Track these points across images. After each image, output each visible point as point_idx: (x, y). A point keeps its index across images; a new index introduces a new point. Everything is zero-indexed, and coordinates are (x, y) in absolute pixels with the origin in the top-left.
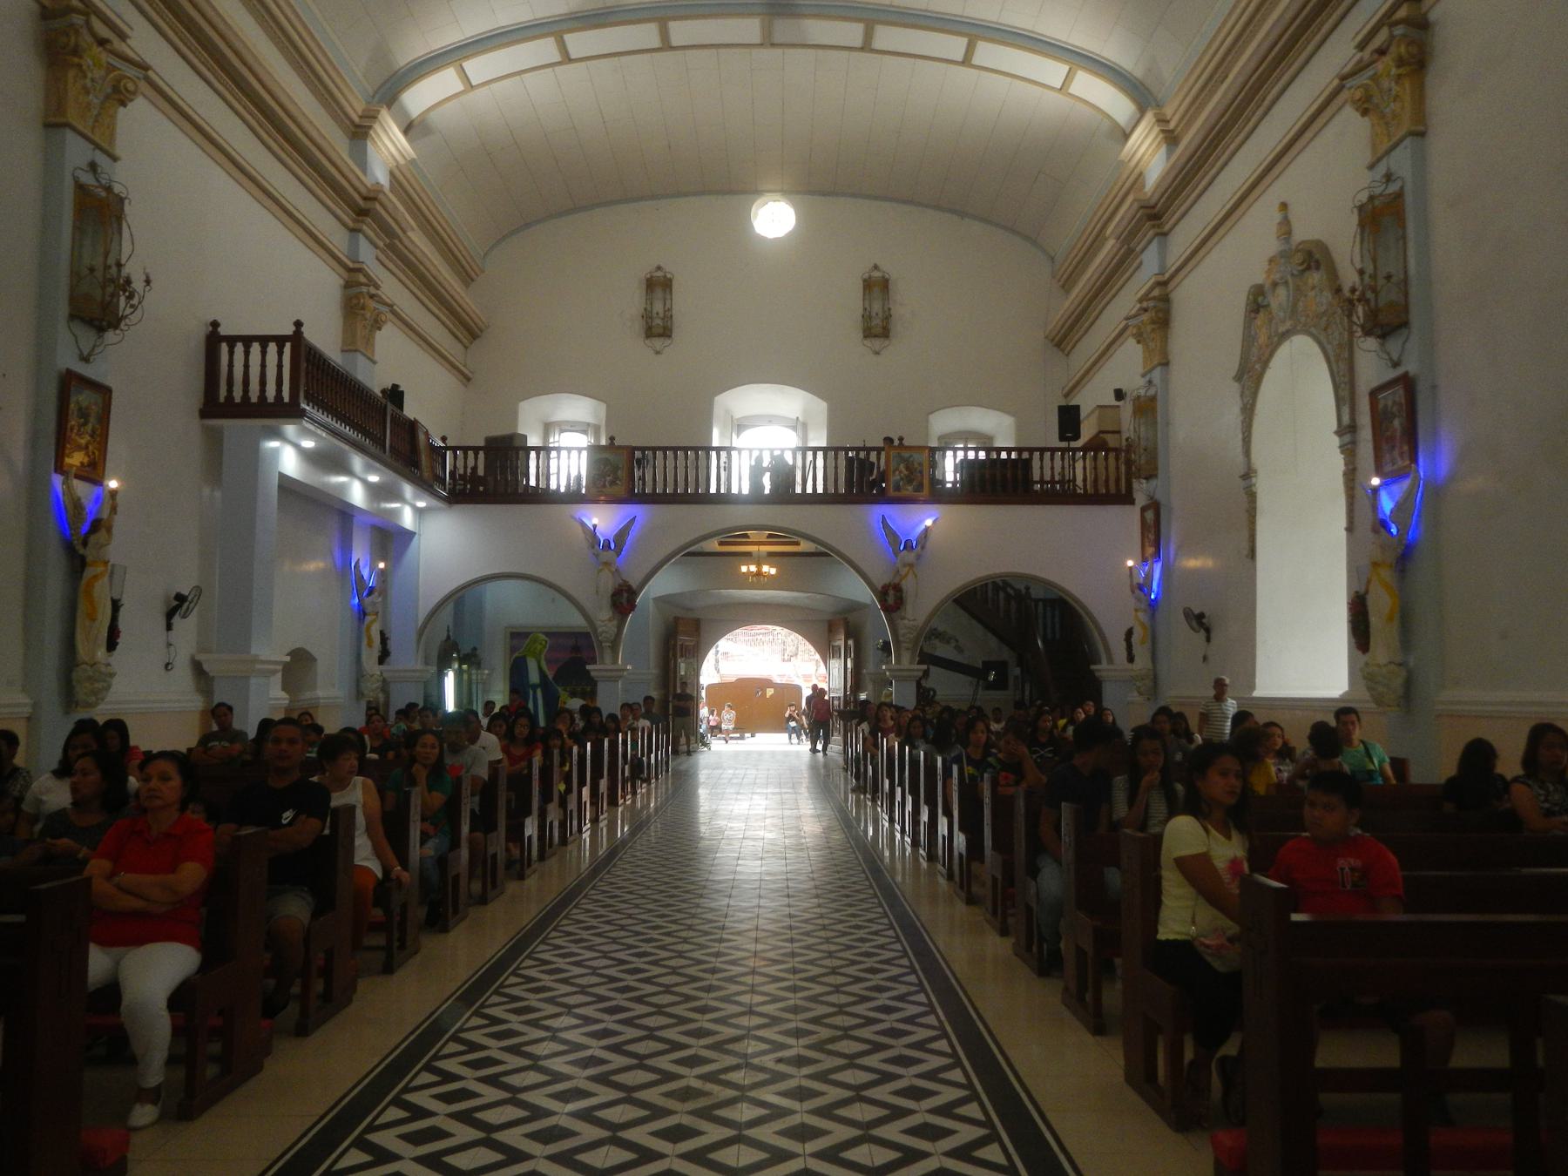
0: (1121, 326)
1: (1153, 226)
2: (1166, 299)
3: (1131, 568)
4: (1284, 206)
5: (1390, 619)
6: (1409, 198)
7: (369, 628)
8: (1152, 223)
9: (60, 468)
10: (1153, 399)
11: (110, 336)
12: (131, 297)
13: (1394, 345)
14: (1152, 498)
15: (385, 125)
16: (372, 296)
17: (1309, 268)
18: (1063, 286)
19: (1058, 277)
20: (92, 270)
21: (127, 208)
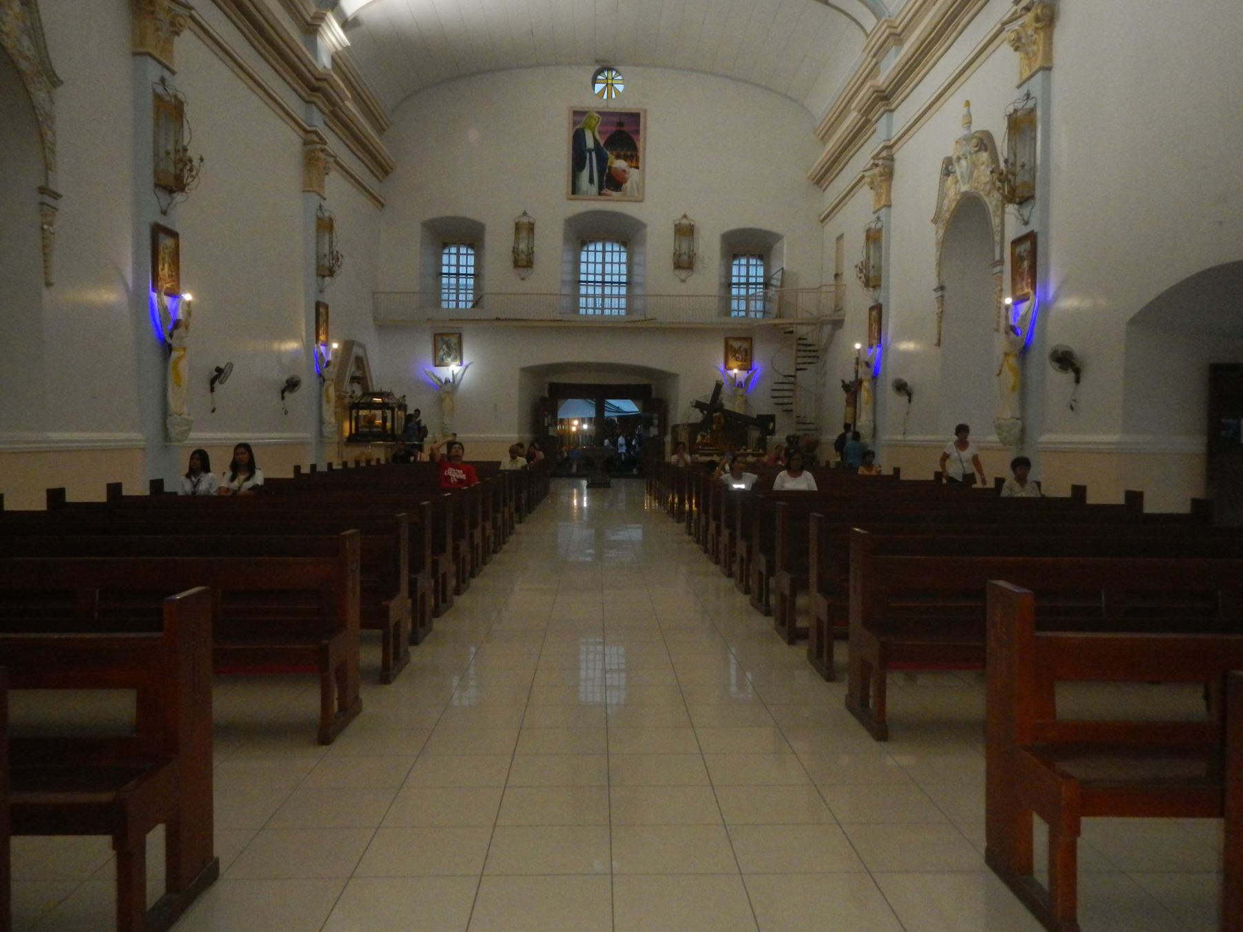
0: (860, 175)
1: (884, 105)
2: (891, 159)
3: (859, 350)
4: (968, 104)
5: (1013, 389)
6: (1039, 113)
7: (327, 390)
8: (883, 102)
9: (155, 288)
10: (879, 231)
11: (179, 197)
12: (191, 170)
13: (1026, 212)
14: (876, 301)
15: (330, 24)
16: (323, 151)
17: (980, 150)
18: (822, 138)
19: (818, 132)
20: (168, 153)
21: (186, 108)
